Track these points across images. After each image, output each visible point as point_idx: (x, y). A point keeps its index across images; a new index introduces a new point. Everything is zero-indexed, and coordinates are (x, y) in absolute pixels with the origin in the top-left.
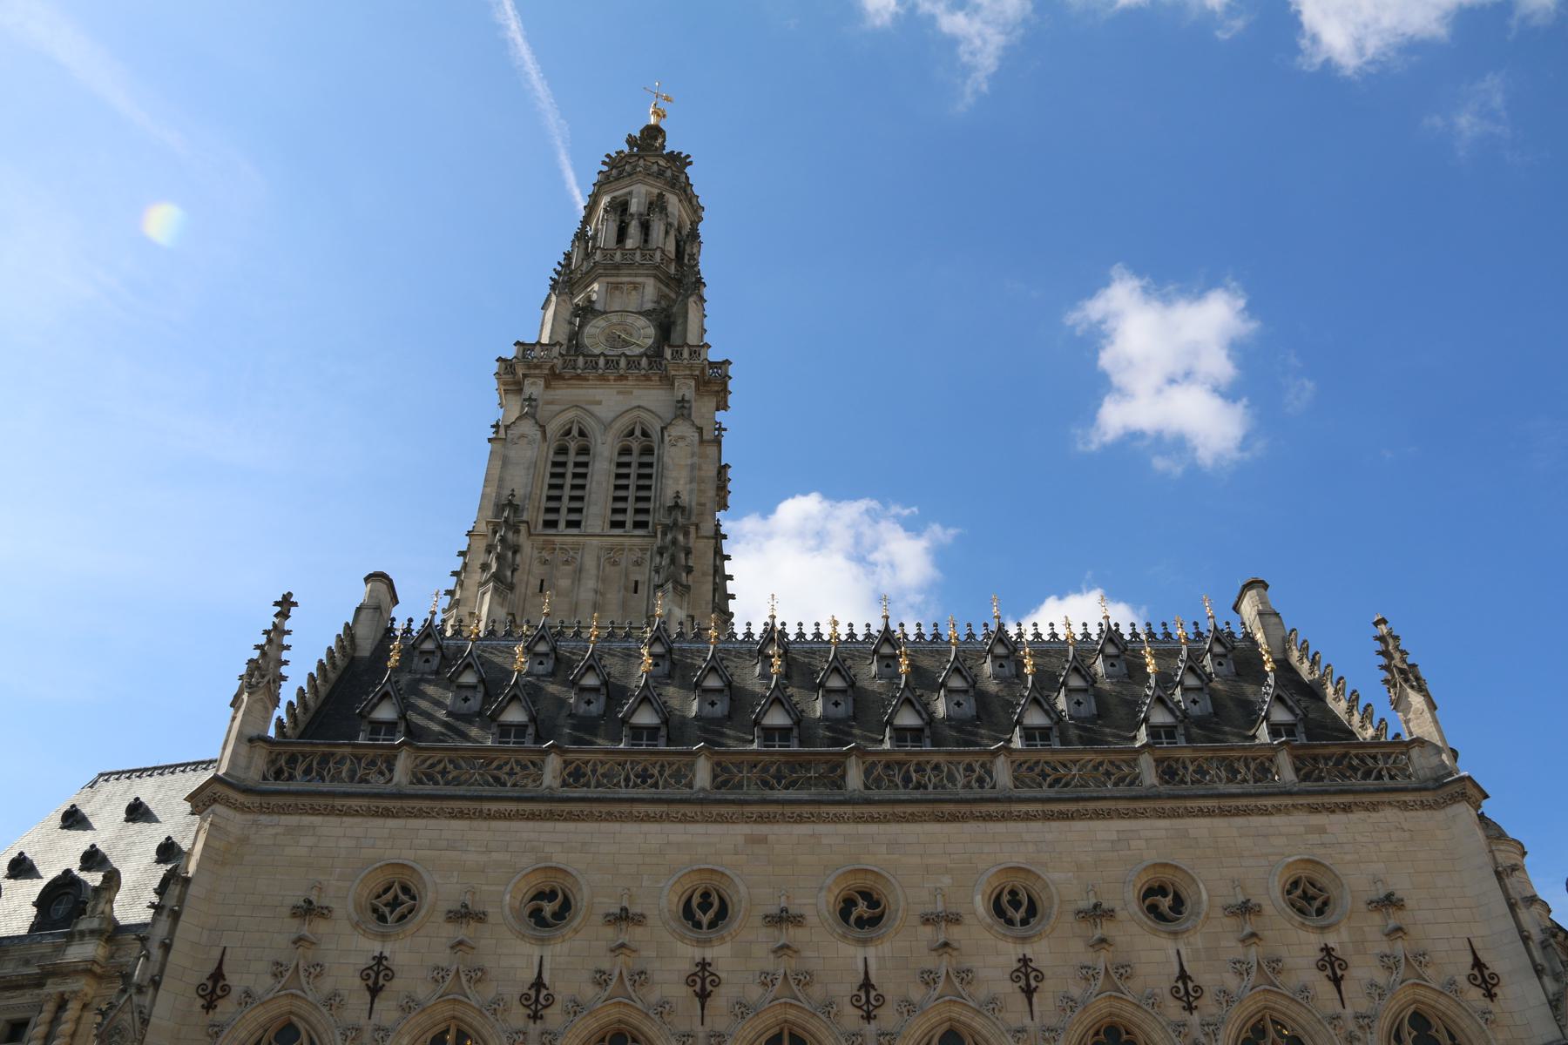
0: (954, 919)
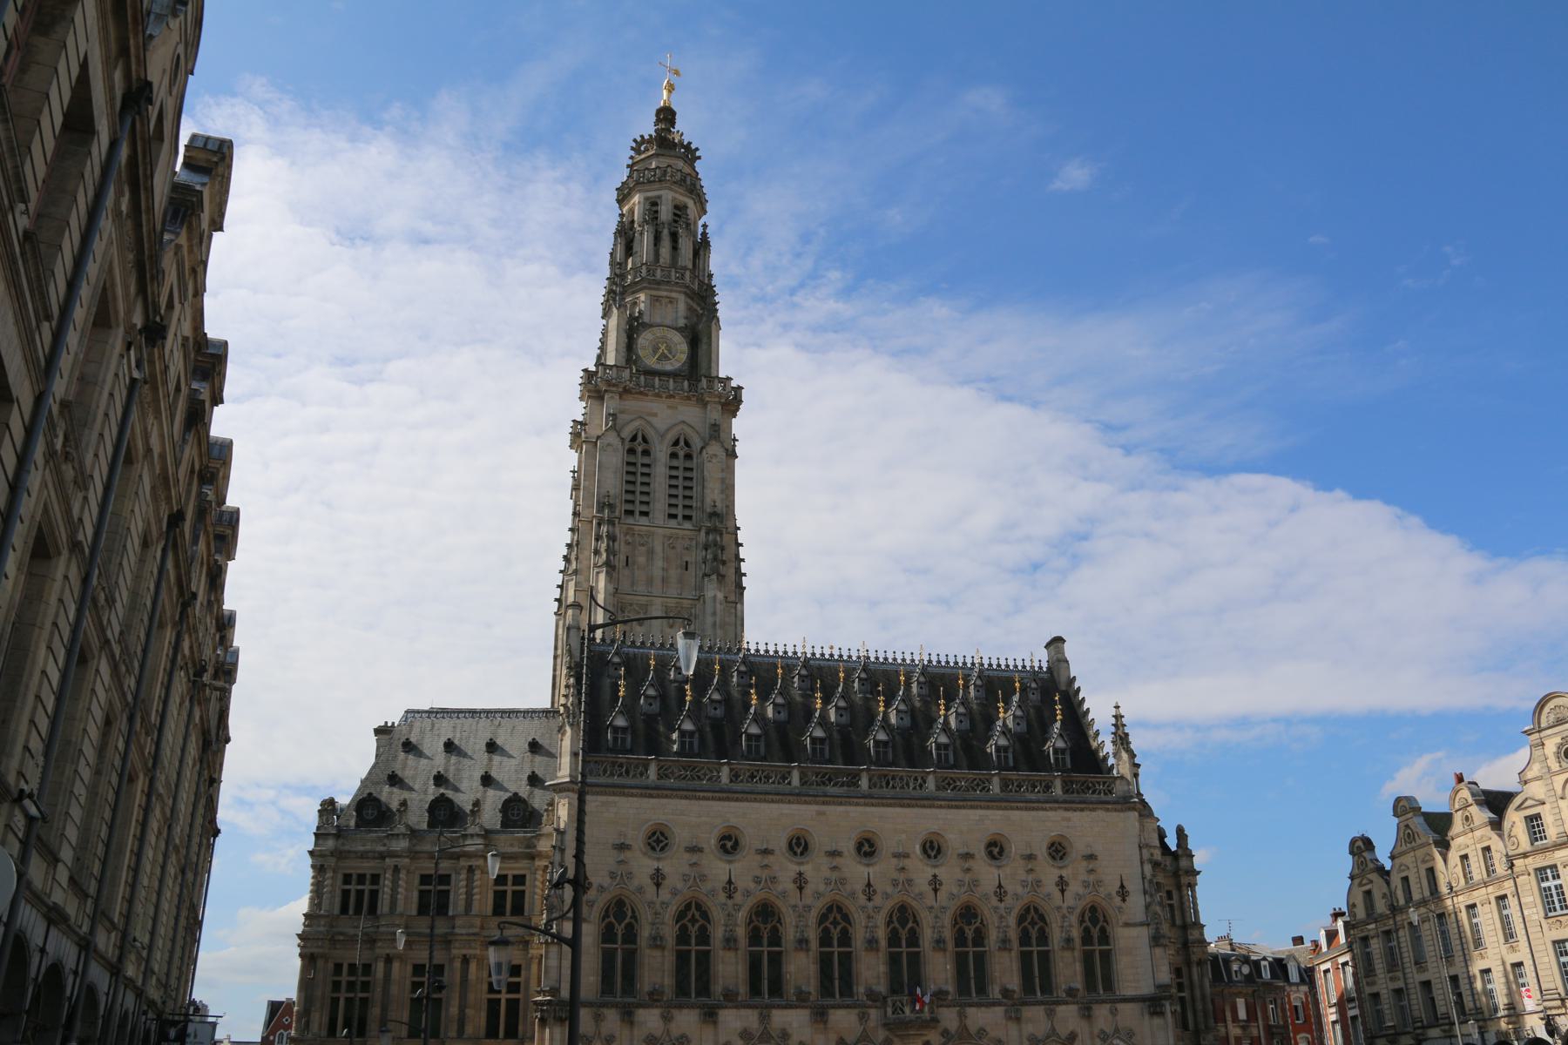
0: (906, 856)
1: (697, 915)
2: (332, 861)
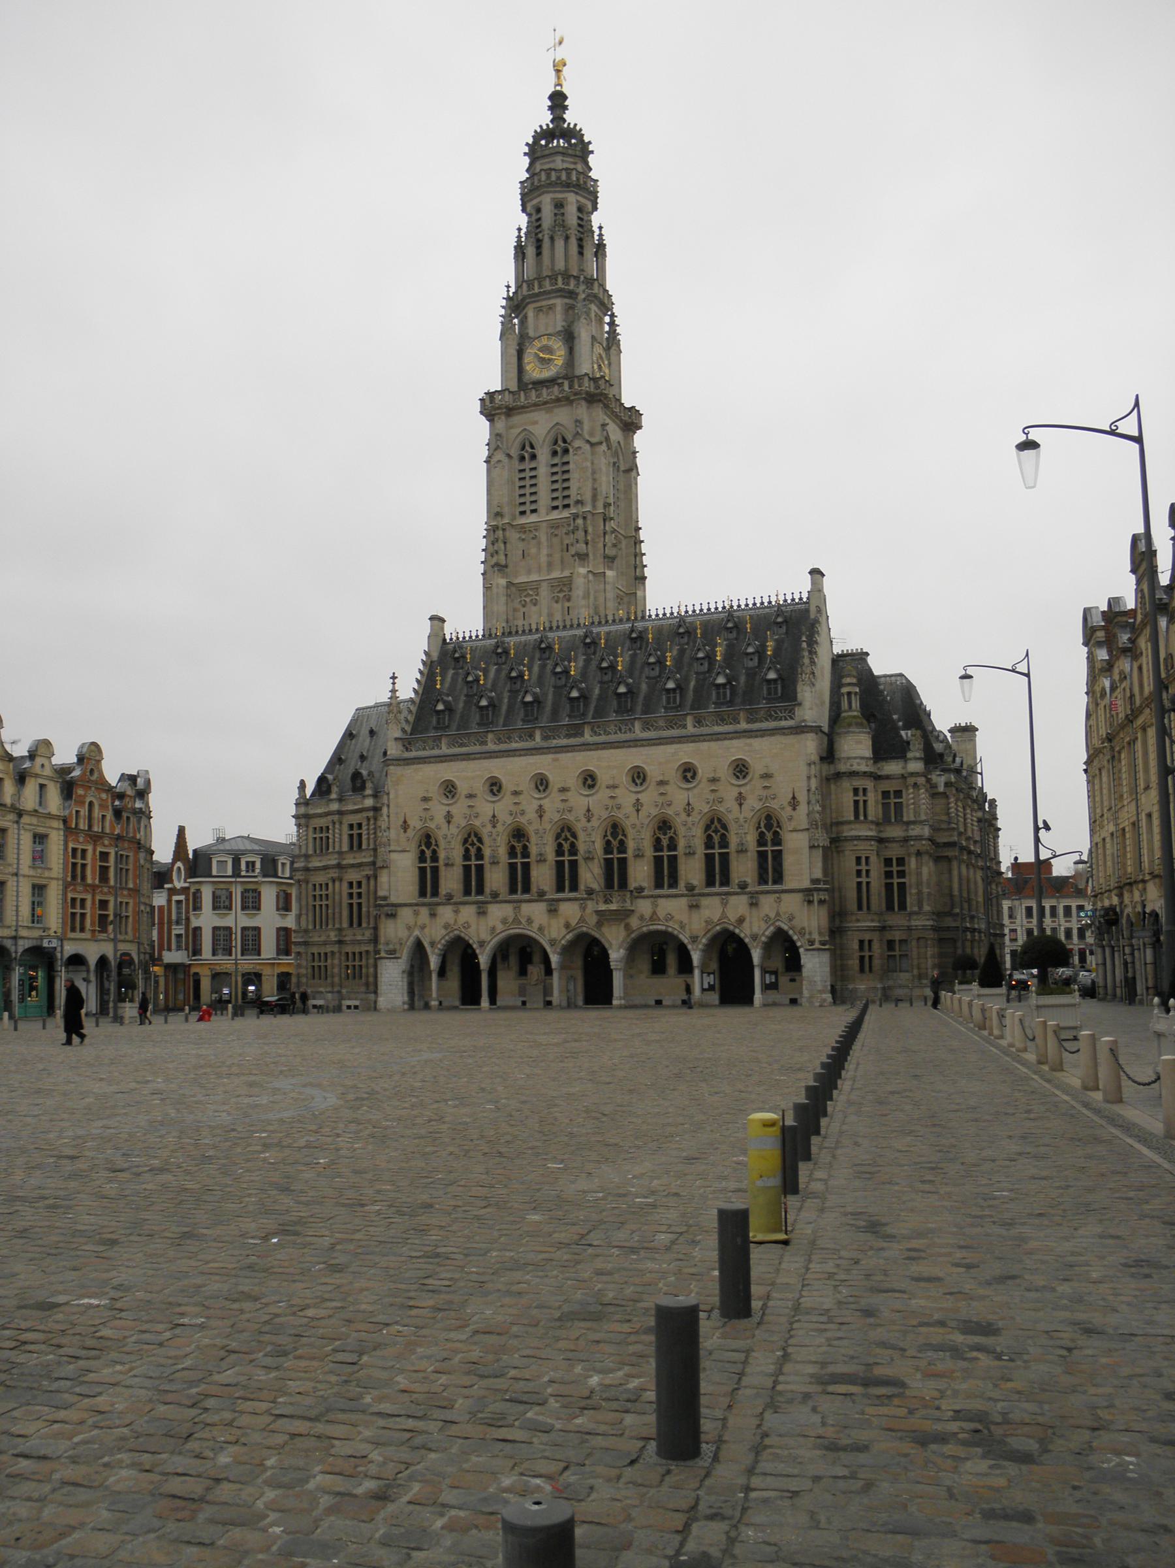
1: (475, 840)
2: (303, 821)
